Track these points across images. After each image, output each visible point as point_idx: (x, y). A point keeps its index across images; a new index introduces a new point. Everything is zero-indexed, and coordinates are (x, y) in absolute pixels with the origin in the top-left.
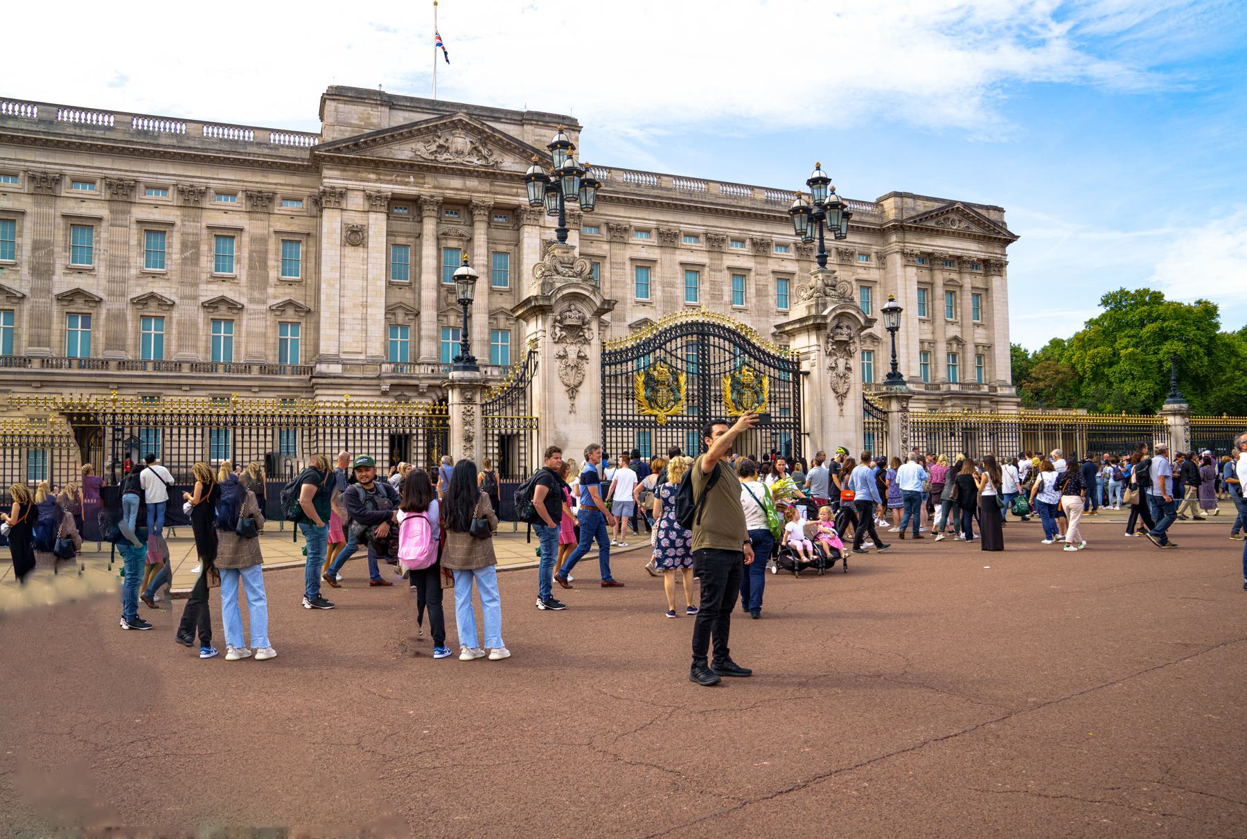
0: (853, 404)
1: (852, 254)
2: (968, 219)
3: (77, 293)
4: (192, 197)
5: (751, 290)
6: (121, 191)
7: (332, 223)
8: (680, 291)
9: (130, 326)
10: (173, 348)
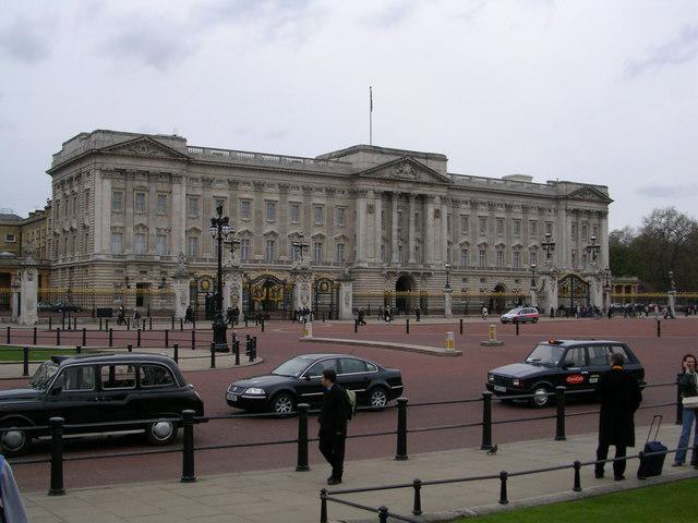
4: (307, 190)
5: (505, 227)
6: (284, 188)
7: (362, 204)
8: (478, 229)
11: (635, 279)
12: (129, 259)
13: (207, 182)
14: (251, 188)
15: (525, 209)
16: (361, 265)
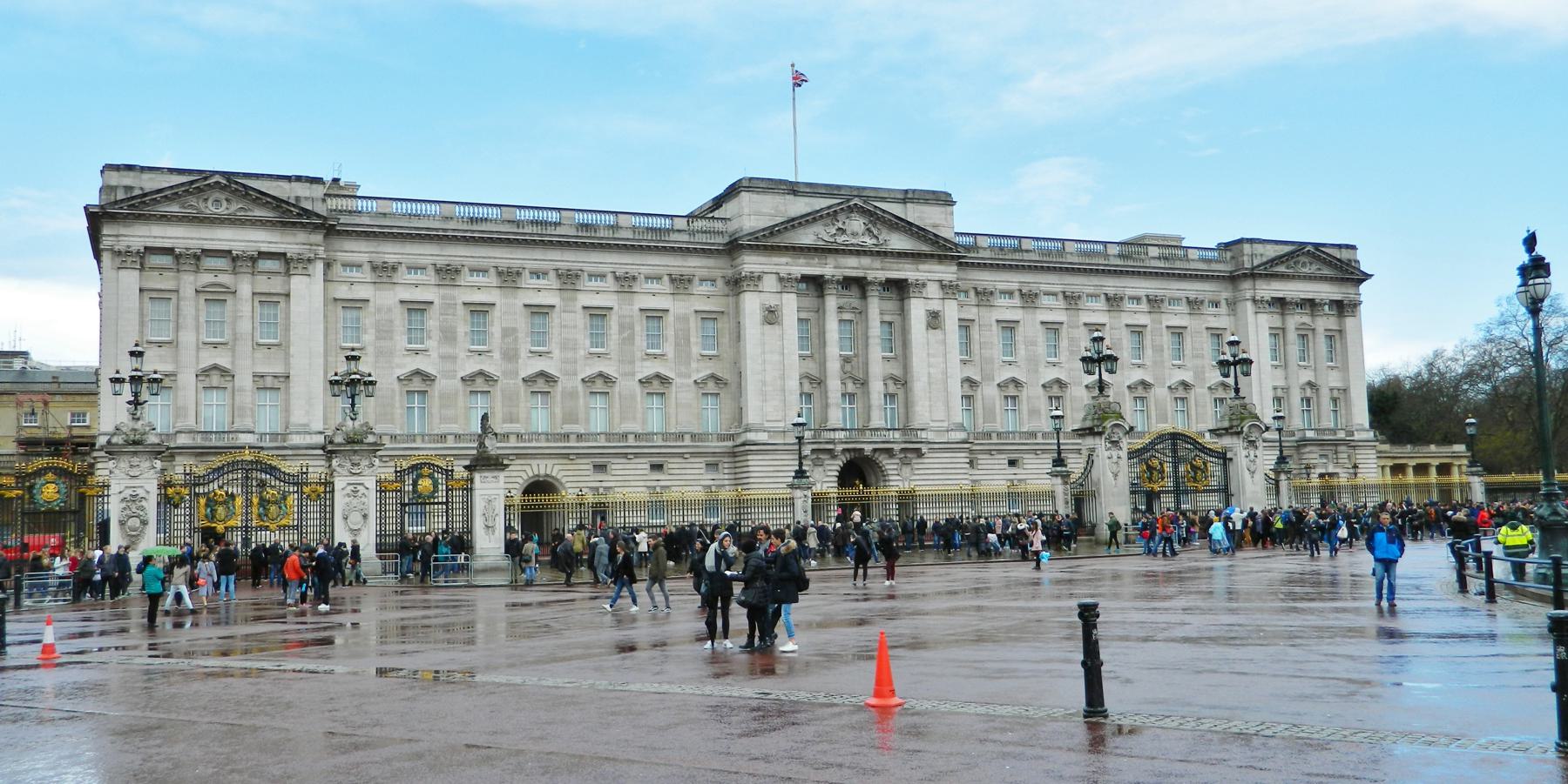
0: (1259, 477)
1: (1202, 302)
2: (1318, 258)
3: (543, 374)
4: (626, 282)
6: (569, 279)
7: (752, 304)
8: (1042, 349)
9: (581, 401)
10: (617, 420)
11: (1460, 448)
12: (183, 440)
13: (384, 271)
14: (492, 279)
15: (1154, 302)
16: (751, 436)
